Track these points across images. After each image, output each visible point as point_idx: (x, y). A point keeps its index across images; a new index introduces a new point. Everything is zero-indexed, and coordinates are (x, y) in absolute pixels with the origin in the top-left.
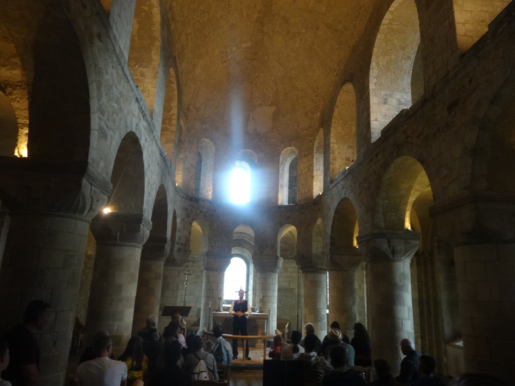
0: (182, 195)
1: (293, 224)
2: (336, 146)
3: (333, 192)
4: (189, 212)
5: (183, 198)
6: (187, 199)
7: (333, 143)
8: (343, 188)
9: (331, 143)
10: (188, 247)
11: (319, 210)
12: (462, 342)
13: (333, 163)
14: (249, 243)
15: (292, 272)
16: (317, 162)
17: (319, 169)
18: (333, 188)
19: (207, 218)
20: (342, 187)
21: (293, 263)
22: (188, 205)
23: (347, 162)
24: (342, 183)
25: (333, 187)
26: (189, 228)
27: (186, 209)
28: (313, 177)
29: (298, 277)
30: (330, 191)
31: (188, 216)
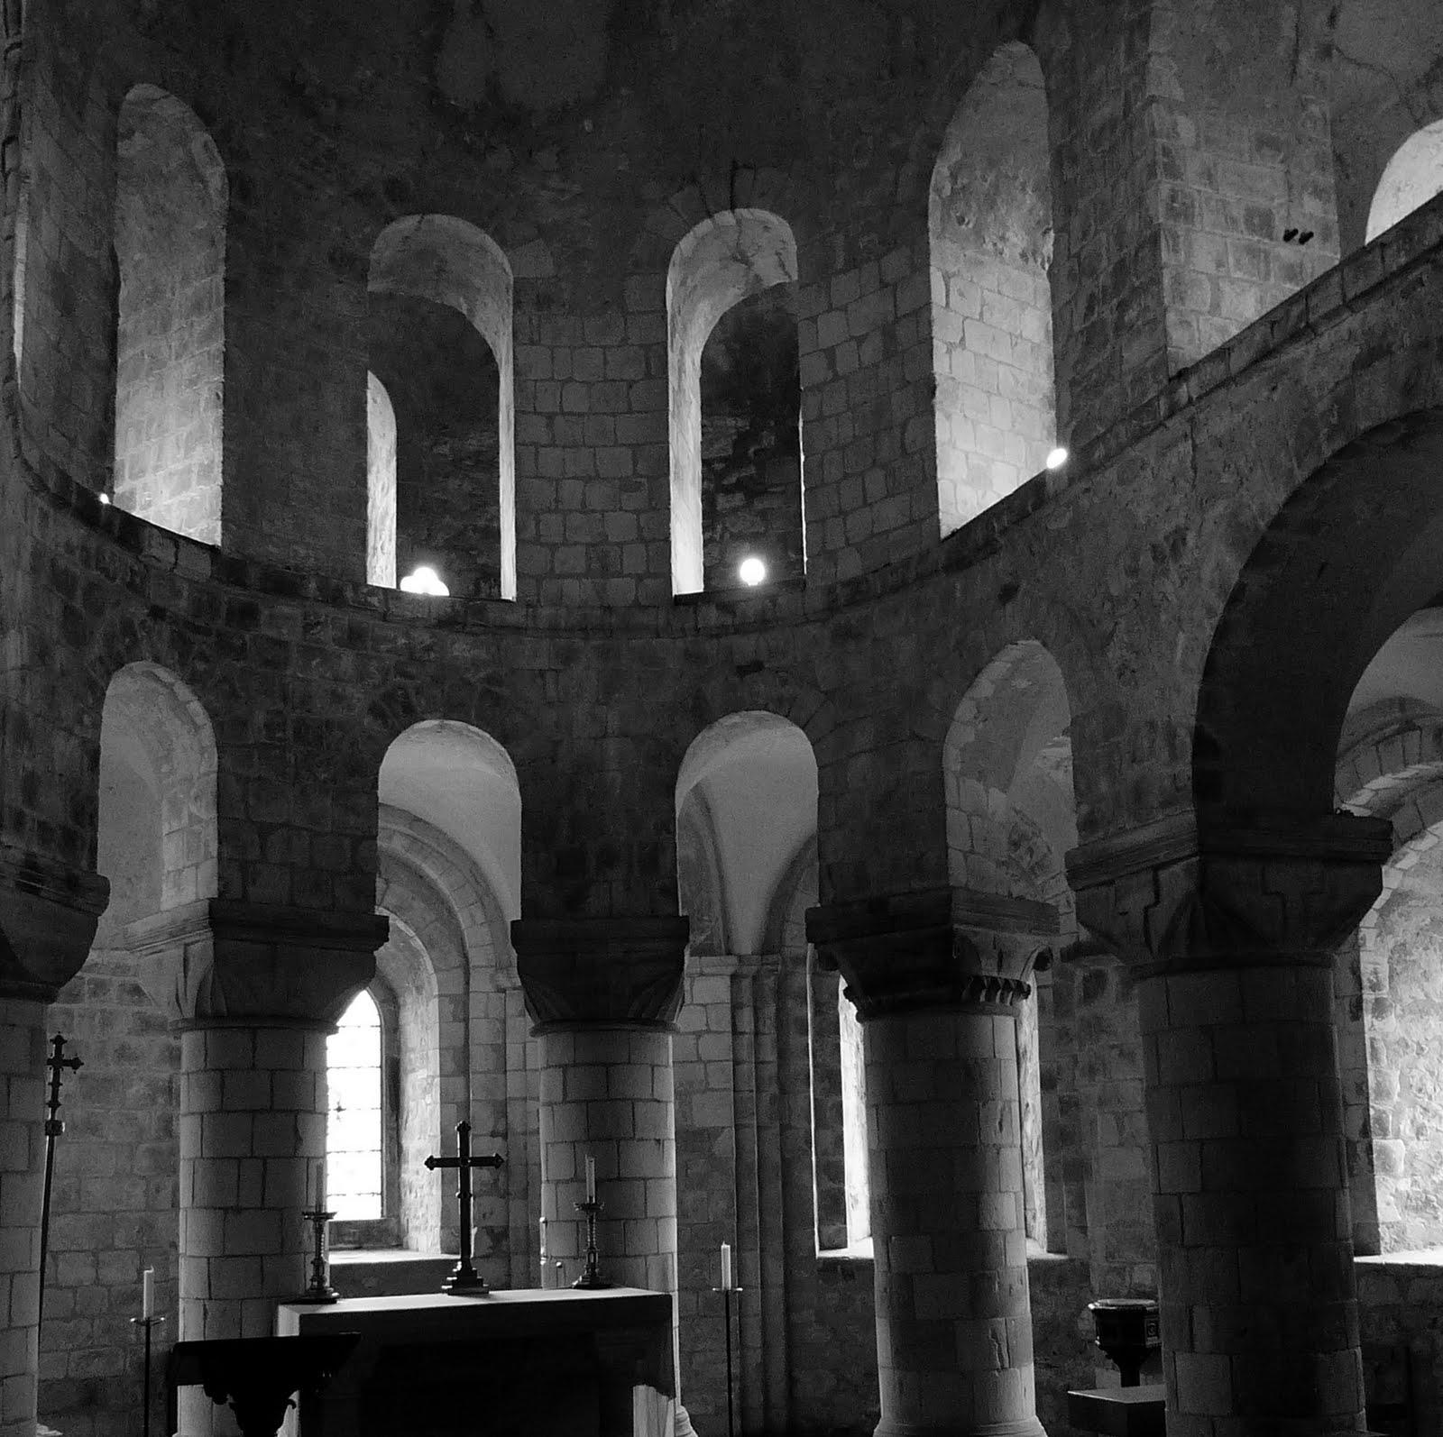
0: (33, 457)
1: (786, 708)
2: (1187, 129)
3: (1219, 422)
4: (78, 604)
5: (40, 485)
6: (60, 501)
7: (1172, 107)
8: (1363, 363)
9: (1153, 99)
10: (84, 863)
11: (1008, 593)
12: (1148, 1343)
13: (1175, 237)
14: (406, 866)
15: (698, 1035)
16: (947, 296)
17: (963, 339)
18: (1222, 393)
19: (201, 666)
20: (1352, 352)
21: (702, 974)
22: (69, 548)
23: (1256, 238)
24: (1374, 312)
25: (1222, 384)
26: (86, 719)
27: (61, 582)
28: (932, 390)
29: (736, 1063)
30: (1177, 424)
31: (76, 633)
